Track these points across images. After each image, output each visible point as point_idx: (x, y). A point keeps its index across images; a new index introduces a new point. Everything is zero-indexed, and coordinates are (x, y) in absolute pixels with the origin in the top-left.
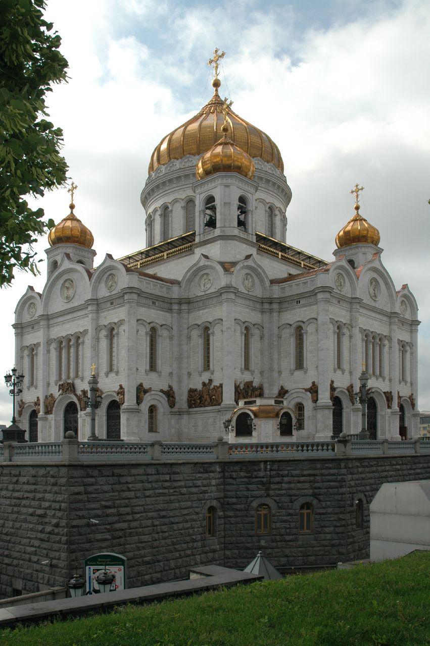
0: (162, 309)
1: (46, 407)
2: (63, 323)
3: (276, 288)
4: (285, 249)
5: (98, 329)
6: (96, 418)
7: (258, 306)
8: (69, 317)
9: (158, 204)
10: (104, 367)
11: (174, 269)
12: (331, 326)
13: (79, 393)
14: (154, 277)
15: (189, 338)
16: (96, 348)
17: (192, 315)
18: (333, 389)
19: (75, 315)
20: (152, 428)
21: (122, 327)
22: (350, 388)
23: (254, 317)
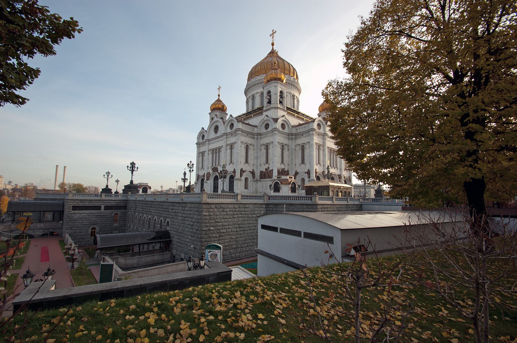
0: (250, 138)
1: (207, 177)
2: (214, 142)
3: (294, 129)
4: (298, 113)
5: (227, 145)
6: (225, 182)
7: (287, 136)
8: (216, 140)
9: (251, 94)
10: (229, 161)
11: (255, 121)
12: (315, 145)
13: (219, 172)
14: (248, 124)
15: (261, 149)
16: (225, 153)
17: (262, 140)
18: (316, 173)
19: (219, 139)
20: (246, 187)
21: (235, 145)
22: (323, 172)
23: (286, 141)
